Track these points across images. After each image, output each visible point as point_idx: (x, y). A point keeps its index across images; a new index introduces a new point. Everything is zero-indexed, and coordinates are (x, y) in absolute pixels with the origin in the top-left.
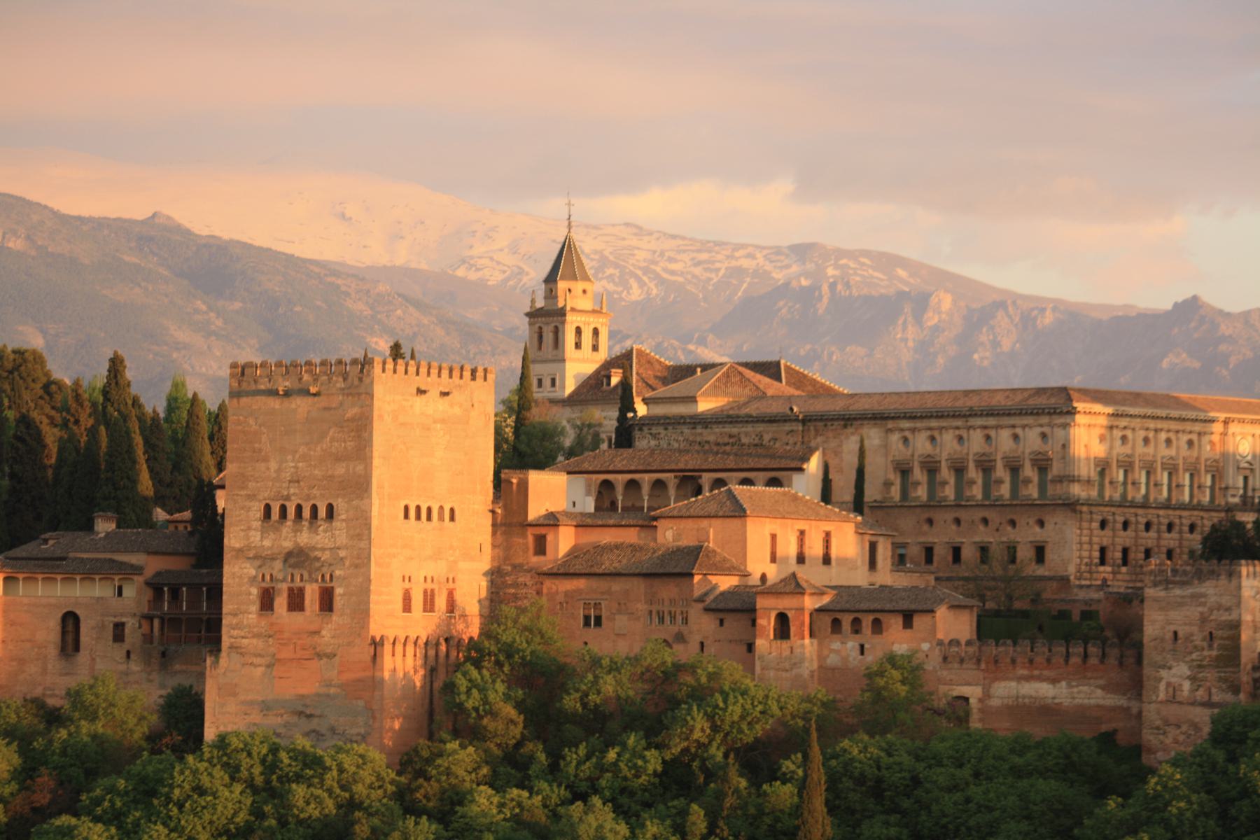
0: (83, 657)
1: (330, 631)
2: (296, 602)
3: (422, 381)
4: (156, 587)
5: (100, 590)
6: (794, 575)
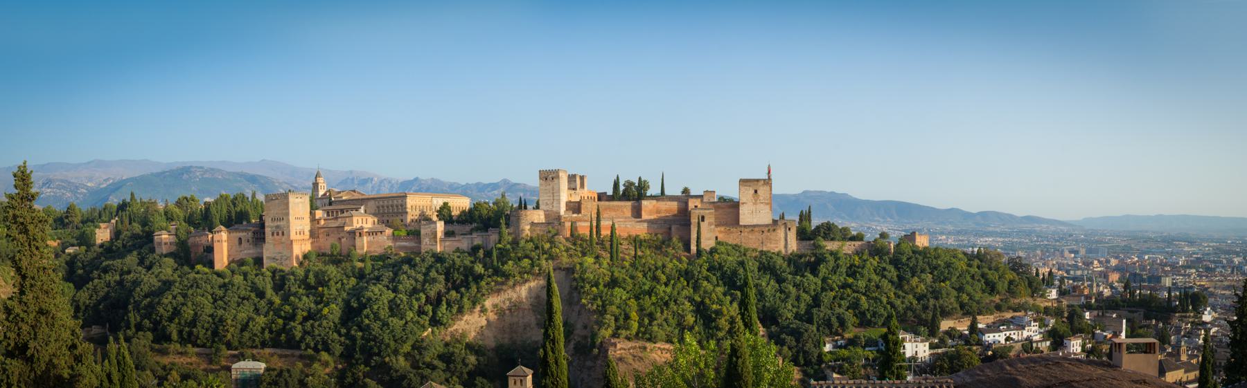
0: (243, 245)
1: (284, 239)
2: (278, 234)
4: (254, 233)
5: (244, 234)
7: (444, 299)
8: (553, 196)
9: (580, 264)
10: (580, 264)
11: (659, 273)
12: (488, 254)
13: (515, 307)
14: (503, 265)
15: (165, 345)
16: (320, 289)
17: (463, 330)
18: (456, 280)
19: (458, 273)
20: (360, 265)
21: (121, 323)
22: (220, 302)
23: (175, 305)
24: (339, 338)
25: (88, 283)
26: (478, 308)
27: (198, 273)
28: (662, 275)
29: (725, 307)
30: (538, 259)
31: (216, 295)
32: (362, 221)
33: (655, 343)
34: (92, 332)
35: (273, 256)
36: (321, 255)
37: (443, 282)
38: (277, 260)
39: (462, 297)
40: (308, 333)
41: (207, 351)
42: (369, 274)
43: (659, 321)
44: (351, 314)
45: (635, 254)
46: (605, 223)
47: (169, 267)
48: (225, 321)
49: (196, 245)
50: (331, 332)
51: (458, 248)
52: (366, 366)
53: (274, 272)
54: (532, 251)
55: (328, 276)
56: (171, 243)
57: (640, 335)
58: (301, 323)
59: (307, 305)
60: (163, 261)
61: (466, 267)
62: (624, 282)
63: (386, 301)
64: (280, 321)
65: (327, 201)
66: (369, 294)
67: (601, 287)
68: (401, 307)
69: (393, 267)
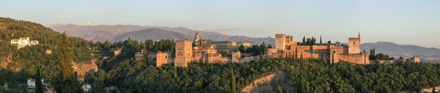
1: (182, 57)
2: (180, 55)
3: (187, 41)
4: (172, 54)
6: (211, 53)
7: (239, 80)
9: (289, 68)
10: (289, 68)
11: (318, 72)
12: (256, 64)
13: (265, 84)
14: (261, 68)
16: (194, 75)
17: (246, 92)
18: (244, 73)
20: (209, 67)
21: (121, 85)
22: (157, 79)
23: (141, 79)
25: (110, 70)
26: (252, 84)
27: (150, 68)
28: (319, 73)
30: (274, 66)
31: (156, 77)
32: (212, 51)
36: (195, 63)
38: (179, 64)
39: (245, 80)
42: (213, 70)
43: (317, 89)
44: (205, 84)
45: (310, 65)
46: (299, 54)
47: (140, 65)
48: (159, 86)
49: (151, 58)
50: (197, 92)
51: (245, 62)
53: (178, 68)
54: (271, 63)
56: (141, 57)
58: (186, 88)
59: (189, 81)
61: (247, 68)
62: (305, 75)
63: (218, 80)
64: (179, 87)
65: (199, 43)
66: (212, 78)
68: (223, 83)
69: (221, 68)
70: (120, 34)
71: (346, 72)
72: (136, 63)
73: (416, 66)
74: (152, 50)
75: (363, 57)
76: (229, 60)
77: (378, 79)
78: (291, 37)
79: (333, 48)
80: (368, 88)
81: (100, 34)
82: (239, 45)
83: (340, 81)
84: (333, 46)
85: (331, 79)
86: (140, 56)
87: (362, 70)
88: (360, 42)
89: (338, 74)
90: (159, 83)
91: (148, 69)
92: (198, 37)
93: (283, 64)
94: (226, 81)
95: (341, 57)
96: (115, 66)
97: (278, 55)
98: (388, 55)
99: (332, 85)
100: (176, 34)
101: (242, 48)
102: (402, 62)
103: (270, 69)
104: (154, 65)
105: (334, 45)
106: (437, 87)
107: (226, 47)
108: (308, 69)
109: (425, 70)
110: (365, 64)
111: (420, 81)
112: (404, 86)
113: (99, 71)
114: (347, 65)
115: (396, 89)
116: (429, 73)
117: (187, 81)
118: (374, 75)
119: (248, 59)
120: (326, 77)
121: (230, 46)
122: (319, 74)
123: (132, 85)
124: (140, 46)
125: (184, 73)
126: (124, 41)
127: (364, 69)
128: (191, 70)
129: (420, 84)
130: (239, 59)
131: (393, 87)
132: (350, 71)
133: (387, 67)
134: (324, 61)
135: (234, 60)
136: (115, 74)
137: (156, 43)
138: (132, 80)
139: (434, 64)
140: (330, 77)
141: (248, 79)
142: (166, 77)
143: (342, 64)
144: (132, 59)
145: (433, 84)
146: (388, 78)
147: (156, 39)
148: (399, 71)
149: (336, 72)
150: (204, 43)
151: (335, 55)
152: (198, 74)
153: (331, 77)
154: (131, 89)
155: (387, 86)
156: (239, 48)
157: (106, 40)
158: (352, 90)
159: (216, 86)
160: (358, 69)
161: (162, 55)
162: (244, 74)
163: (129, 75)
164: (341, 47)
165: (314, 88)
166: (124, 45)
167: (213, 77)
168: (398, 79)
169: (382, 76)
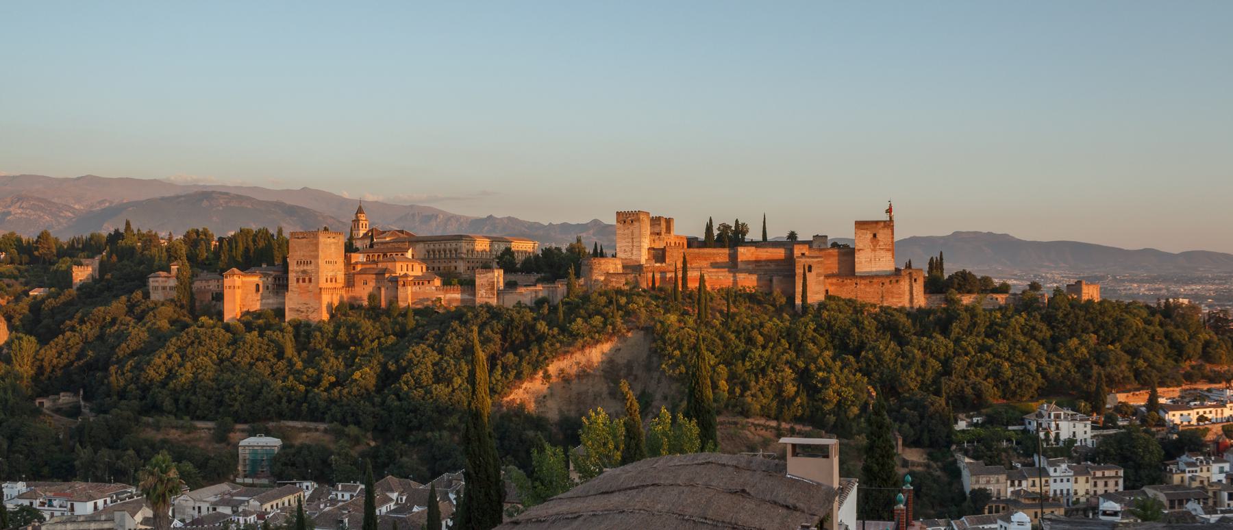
2: (304, 281)
4: (275, 278)
7: (499, 362)
8: (633, 242)
9: (660, 322)
10: (660, 322)
12: (553, 309)
13: (583, 374)
14: (570, 323)
15: (157, 417)
16: (352, 348)
18: (515, 340)
19: (517, 332)
20: (400, 319)
22: (226, 363)
23: (169, 366)
24: (372, 409)
26: (541, 374)
27: (202, 326)
29: (833, 375)
30: (613, 317)
31: (223, 355)
32: (409, 267)
33: (748, 418)
34: (60, 401)
35: (298, 307)
36: (353, 306)
37: (499, 342)
38: (302, 312)
39: (520, 361)
40: (335, 402)
41: (210, 425)
42: (412, 330)
44: (387, 378)
45: (728, 310)
46: (693, 274)
48: (232, 387)
49: (203, 292)
50: (362, 402)
51: (519, 302)
52: (404, 443)
53: (297, 326)
54: (604, 307)
55: (363, 332)
56: (171, 288)
57: (730, 408)
58: (326, 390)
59: (335, 368)
60: (159, 310)
61: (526, 322)
63: (429, 364)
64: (302, 388)
65: (368, 242)
66: (410, 355)
67: (685, 351)
68: (448, 371)
69: (441, 324)
70: (94, 209)
71: (847, 333)
72: (152, 309)
73: (1087, 312)
74: (210, 264)
75: (902, 283)
76: (466, 297)
77: (956, 358)
78: (669, 221)
79: (803, 254)
80: (923, 386)
81: (19, 208)
82: (499, 246)
83: (830, 362)
84: (805, 249)
85: (797, 357)
86: (166, 284)
87: (901, 327)
88: (893, 234)
89: (822, 341)
90: (231, 376)
91: (195, 331)
92: (364, 223)
93: (642, 309)
94: (455, 365)
95: (832, 284)
96: (75, 322)
97: (626, 279)
98: (987, 277)
99: (804, 377)
100: (292, 211)
101: (508, 257)
102: (1036, 300)
103: (601, 325)
104: (214, 317)
105: (807, 246)
106: (1165, 389)
107: (456, 255)
108: (722, 324)
109: (1119, 329)
110: (912, 308)
111: (1103, 365)
112: (1044, 381)
113: (12, 341)
114: (850, 312)
115: (1018, 391)
116: (1136, 339)
117: (327, 369)
118: (942, 344)
119: (527, 293)
120: (781, 350)
121: (468, 251)
122: (760, 339)
123: (140, 385)
124: (164, 250)
125: (318, 342)
126: (110, 234)
127: (909, 323)
128: (343, 331)
129: (1103, 376)
130: (498, 294)
131: (1005, 384)
132: (861, 329)
133: (984, 316)
134: (774, 299)
135: (483, 296)
136: (74, 350)
137: (221, 240)
138: (135, 367)
139: (1151, 307)
140: (797, 351)
141: (527, 357)
142: (255, 357)
143: (833, 306)
144: (138, 295)
145: (1149, 376)
146: (988, 356)
147: (222, 228)
148: (1026, 330)
149: (815, 334)
150: (383, 240)
151: (811, 277)
152: (363, 343)
153: (799, 349)
154: (134, 401)
155: (985, 382)
156: (498, 258)
157: (41, 229)
158: (869, 394)
159: (425, 384)
160: (888, 323)
161: (243, 282)
162: (517, 342)
163: (128, 351)
164: (831, 251)
165: (744, 387)
166: (108, 247)
167: (414, 352)
168: (1024, 358)
169: (970, 348)
